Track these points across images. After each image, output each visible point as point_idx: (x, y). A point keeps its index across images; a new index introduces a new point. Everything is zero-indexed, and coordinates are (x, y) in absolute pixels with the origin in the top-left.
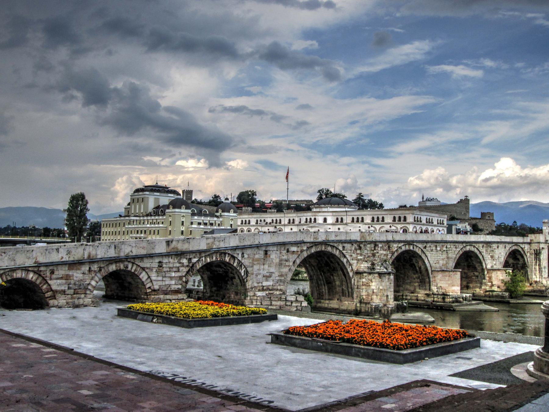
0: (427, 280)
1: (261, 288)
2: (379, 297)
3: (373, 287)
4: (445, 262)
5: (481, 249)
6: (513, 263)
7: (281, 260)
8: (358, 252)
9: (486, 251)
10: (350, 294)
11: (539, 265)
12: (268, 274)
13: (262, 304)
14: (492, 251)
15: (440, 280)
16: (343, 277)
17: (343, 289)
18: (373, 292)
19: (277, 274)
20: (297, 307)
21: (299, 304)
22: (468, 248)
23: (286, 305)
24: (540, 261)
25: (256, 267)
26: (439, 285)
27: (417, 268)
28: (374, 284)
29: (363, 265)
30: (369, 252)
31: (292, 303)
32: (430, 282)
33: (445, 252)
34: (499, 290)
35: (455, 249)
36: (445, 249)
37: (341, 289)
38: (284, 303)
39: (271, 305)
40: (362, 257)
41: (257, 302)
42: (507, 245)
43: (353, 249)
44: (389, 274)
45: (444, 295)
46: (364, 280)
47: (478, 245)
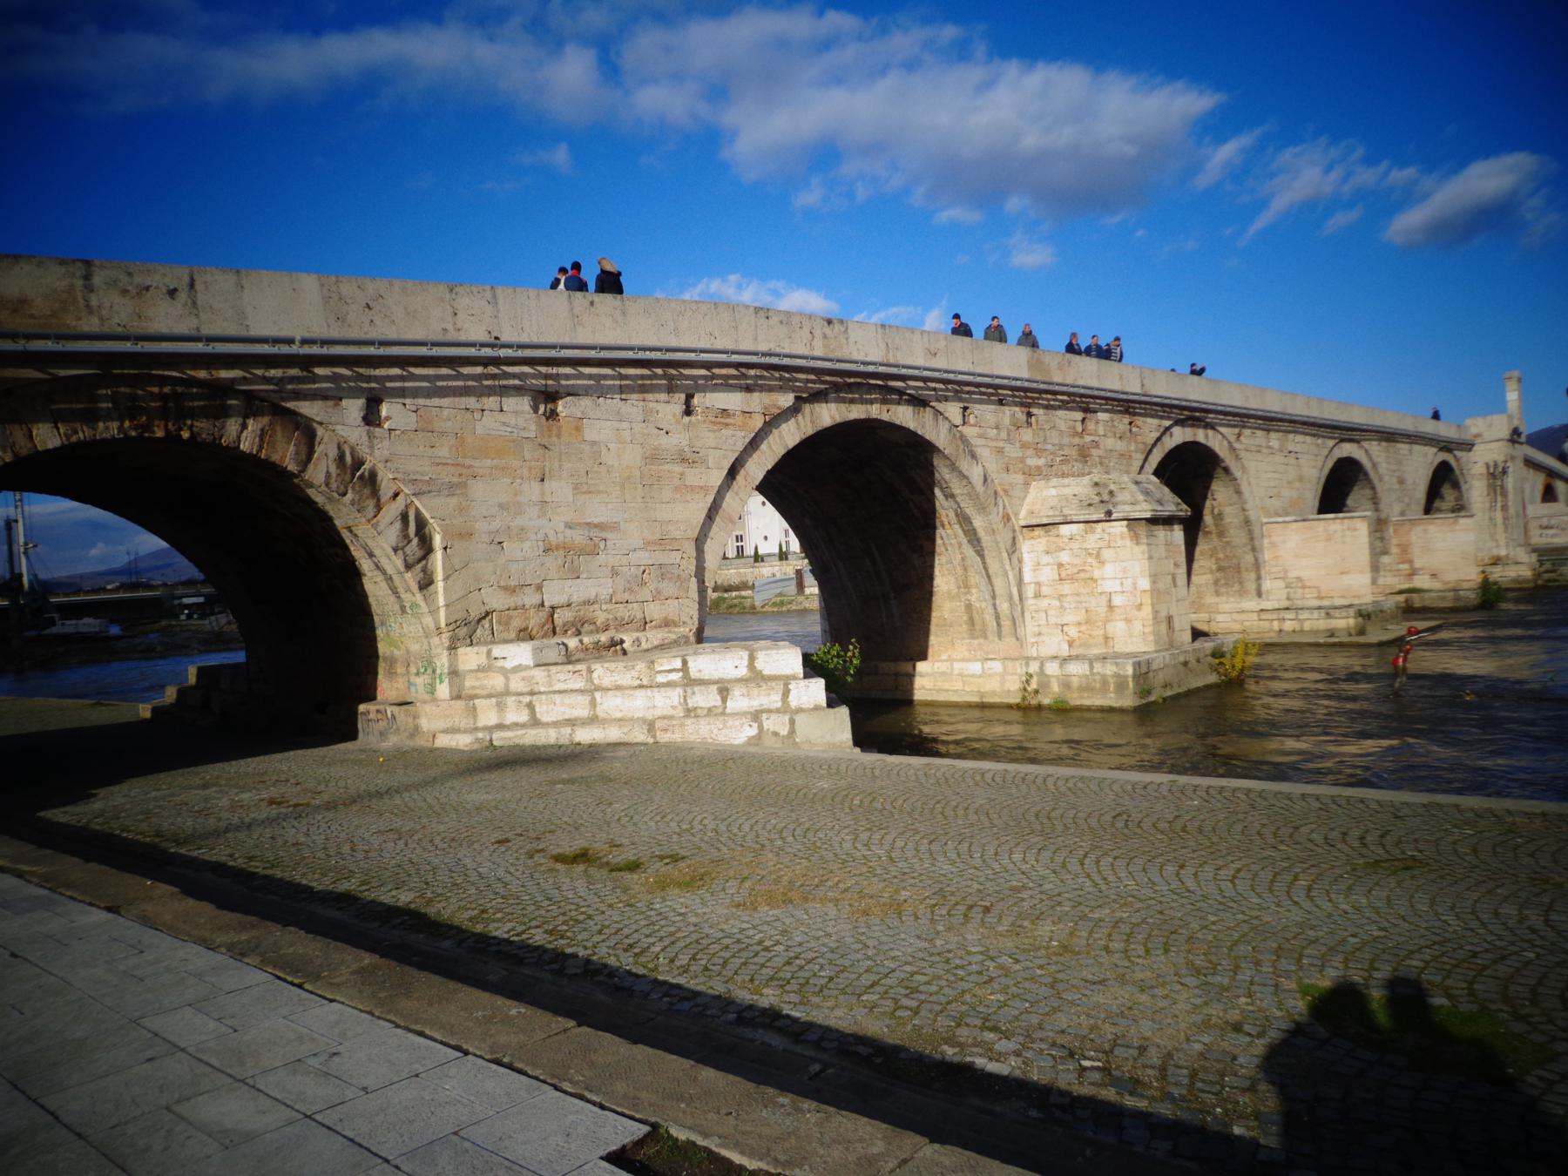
0: (1249, 558)
1: (535, 620)
3: (1109, 586)
7: (653, 457)
8: (1027, 435)
10: (1006, 623)
11: (1504, 508)
12: (578, 537)
13: (535, 722)
16: (969, 552)
17: (969, 607)
18: (1111, 607)
19: (634, 533)
20: (756, 716)
21: (774, 700)
22: (1348, 450)
23: (690, 712)
24: (1504, 494)
25: (486, 494)
26: (1293, 574)
28: (1109, 569)
29: (1053, 492)
30: (1066, 440)
31: (724, 692)
32: (1257, 565)
34: (1436, 585)
37: (960, 605)
38: (675, 696)
39: (593, 720)
40: (1041, 462)
43: (1007, 421)
44: (1167, 521)
46: (1065, 557)
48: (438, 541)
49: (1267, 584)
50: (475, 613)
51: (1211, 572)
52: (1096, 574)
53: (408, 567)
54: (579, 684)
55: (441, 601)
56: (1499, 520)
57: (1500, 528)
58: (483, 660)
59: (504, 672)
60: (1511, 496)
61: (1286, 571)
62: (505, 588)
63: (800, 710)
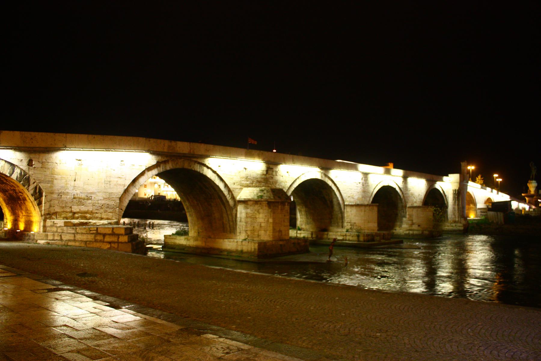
0: (340, 215)
2: (268, 232)
3: (261, 220)
13: (61, 240)
18: (261, 226)
20: (110, 243)
23: (96, 241)
41: (54, 235)
48: (44, 194)
49: (345, 224)
50: (52, 211)
52: (257, 216)
53: (35, 200)
54: (73, 232)
55: (43, 209)
58: (52, 224)
59: (57, 227)
62: (61, 207)
63: (121, 243)
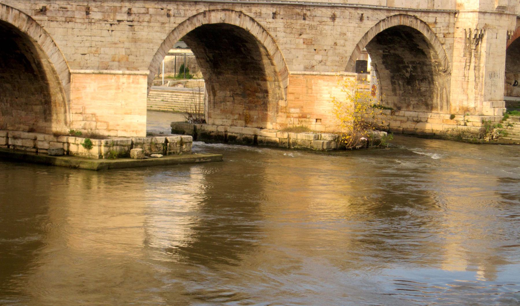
4: (122, 52)
5: (267, 22)
6: (412, 63)
9: (287, 26)
11: (477, 68)
14: (311, 27)
15: (93, 98)
24: (478, 57)
26: (89, 111)
27: (34, 66)
33: (124, 26)
35: (165, 19)
36: (125, 17)
42: (367, 13)
45: (90, 138)
47: (254, 9)
51: (42, 104)
56: (472, 78)
57: (471, 85)
60: (483, 59)
61: (84, 108)
